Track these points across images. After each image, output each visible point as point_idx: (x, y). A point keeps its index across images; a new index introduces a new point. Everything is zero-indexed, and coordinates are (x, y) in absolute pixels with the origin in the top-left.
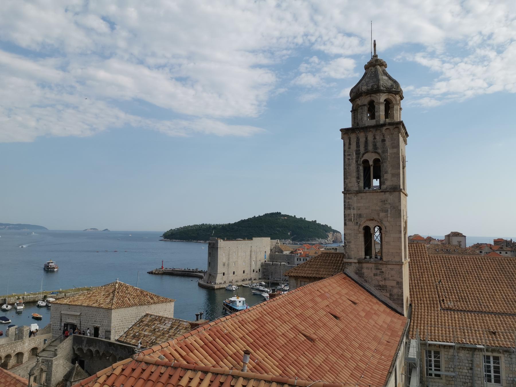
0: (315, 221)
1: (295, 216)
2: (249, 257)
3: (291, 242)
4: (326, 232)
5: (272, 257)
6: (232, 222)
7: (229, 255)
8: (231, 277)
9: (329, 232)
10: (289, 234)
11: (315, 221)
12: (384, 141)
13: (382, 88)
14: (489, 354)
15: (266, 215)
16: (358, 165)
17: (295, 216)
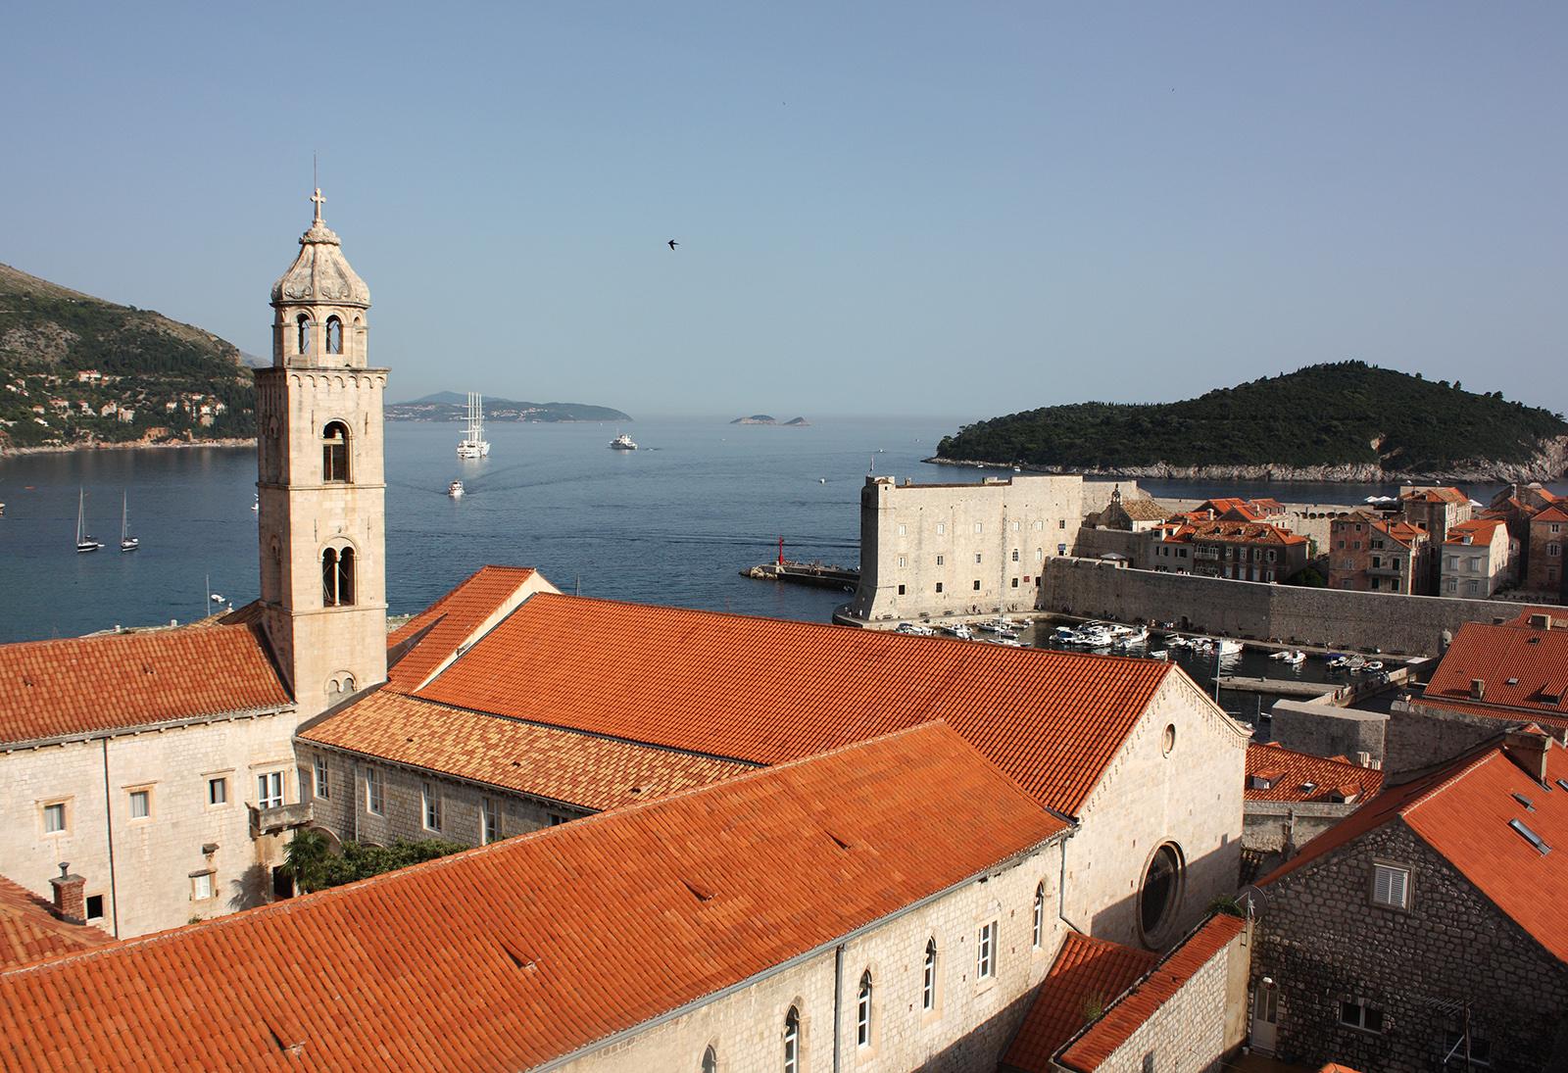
0: (1499, 395)
1: (1419, 375)
2: (997, 540)
3: (1379, 474)
4: (1538, 436)
5: (1087, 541)
6: (1169, 398)
7: (920, 531)
8: (931, 601)
9: (1551, 437)
10: (1375, 444)
11: (1499, 395)
12: (280, 396)
13: (285, 298)
14: (372, 766)
15: (1305, 372)
16: (267, 437)
17: (1419, 375)
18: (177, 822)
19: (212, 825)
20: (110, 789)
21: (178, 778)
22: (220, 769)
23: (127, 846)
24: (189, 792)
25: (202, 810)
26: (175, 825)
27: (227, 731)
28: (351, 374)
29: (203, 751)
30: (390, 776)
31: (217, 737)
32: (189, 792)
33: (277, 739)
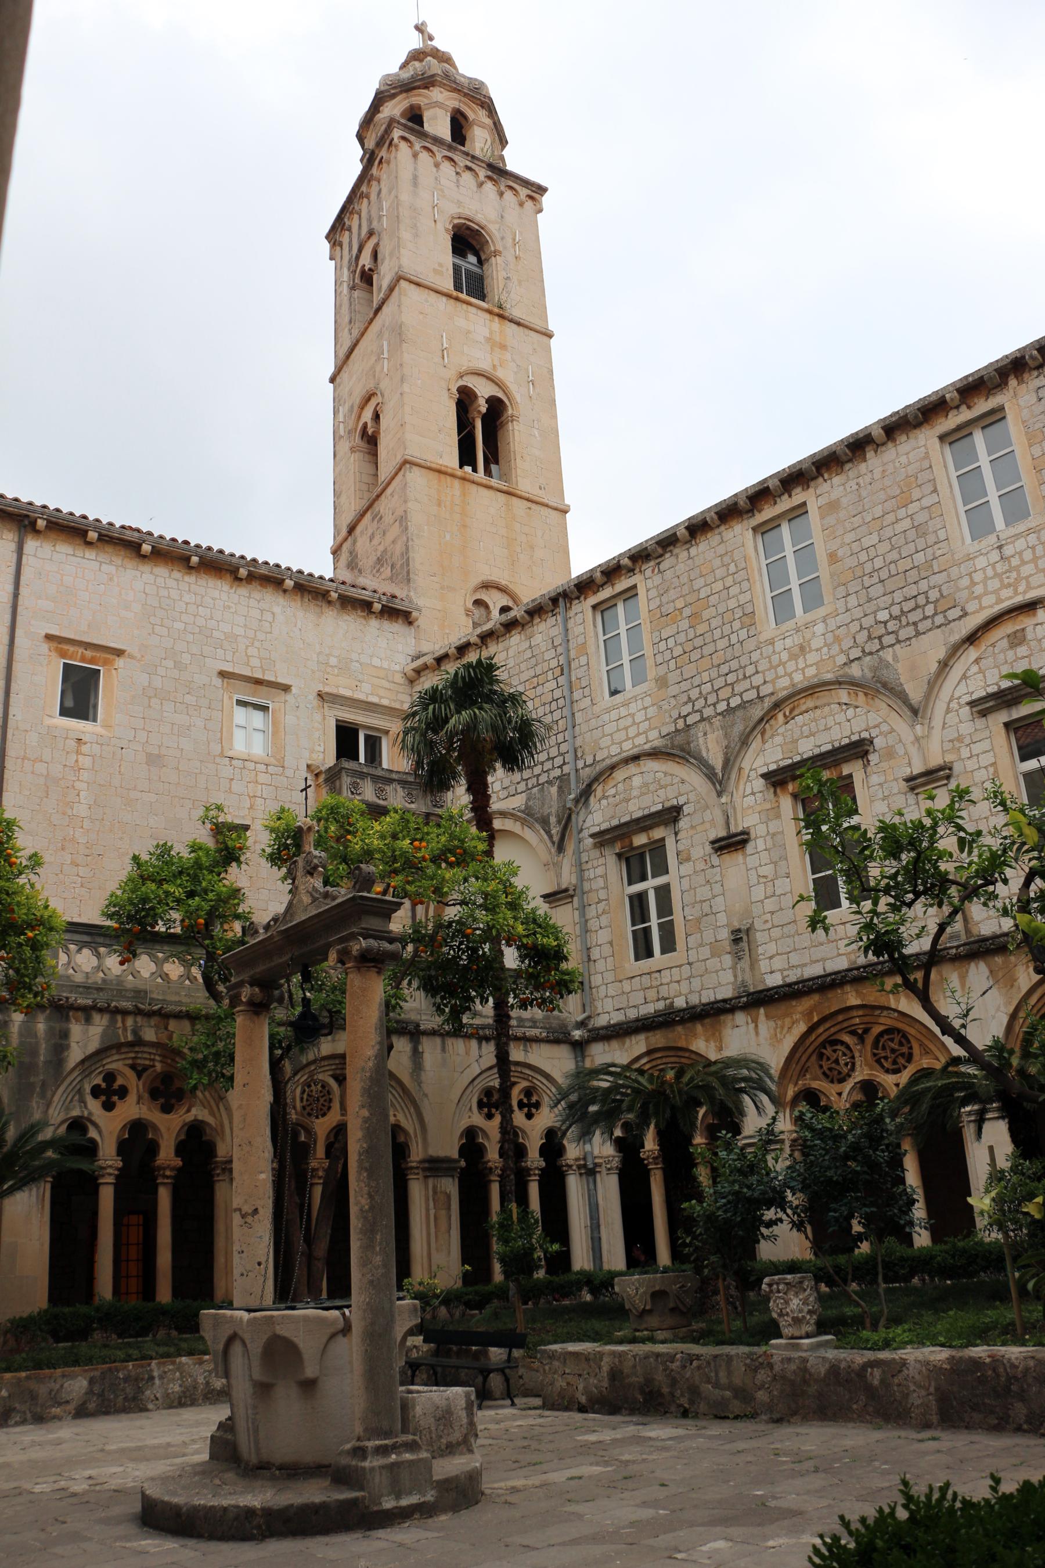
18: (159, 756)
19: (236, 787)
20: (19, 632)
21: (170, 664)
22: (258, 675)
23: (41, 768)
24: (188, 699)
25: (216, 749)
26: (154, 760)
27: (277, 610)
28: (490, 173)
29: (226, 628)
30: (657, 579)
31: (256, 613)
32: (188, 699)
33: (376, 662)
